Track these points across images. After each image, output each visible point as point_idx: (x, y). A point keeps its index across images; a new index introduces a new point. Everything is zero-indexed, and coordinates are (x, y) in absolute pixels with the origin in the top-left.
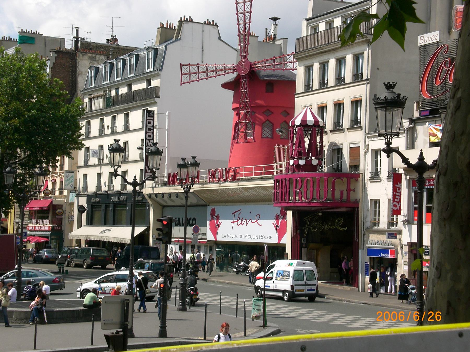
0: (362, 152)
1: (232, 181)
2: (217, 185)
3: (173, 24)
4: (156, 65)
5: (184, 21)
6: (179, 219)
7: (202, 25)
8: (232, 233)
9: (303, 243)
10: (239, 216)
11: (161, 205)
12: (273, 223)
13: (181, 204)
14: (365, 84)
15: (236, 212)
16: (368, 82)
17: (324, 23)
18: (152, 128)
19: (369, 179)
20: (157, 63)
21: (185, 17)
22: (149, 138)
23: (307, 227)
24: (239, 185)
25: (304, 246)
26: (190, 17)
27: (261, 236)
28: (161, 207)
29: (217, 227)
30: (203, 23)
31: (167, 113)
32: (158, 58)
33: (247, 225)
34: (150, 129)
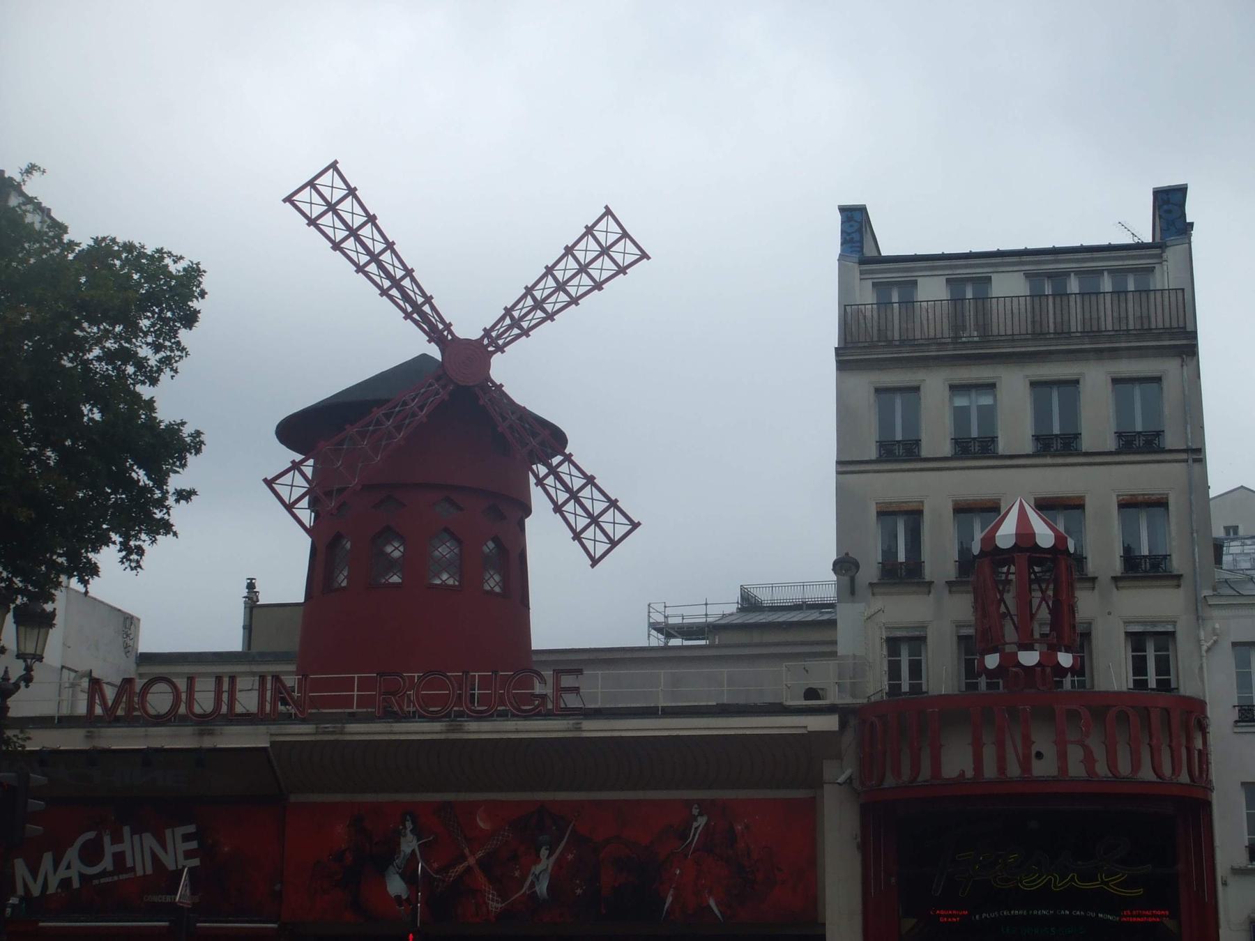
17: (944, 278)
24: (580, 729)
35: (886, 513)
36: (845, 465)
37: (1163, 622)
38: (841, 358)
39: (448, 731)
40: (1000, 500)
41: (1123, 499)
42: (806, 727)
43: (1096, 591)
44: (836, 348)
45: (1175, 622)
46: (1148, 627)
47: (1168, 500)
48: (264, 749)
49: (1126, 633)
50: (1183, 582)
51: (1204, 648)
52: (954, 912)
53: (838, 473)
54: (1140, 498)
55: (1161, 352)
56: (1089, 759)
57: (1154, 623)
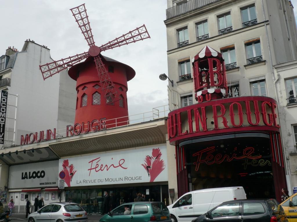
1: (96, 131)
2: (78, 137)
3: (17, 49)
4: (7, 66)
6: (26, 173)
7: (40, 47)
8: (88, 178)
9: (189, 178)
10: (97, 163)
11: (7, 164)
12: (143, 165)
13: (29, 161)
14: (264, 25)
15: (93, 160)
18: (5, 104)
21: (29, 39)
24: (106, 134)
25: (190, 181)
27: (126, 178)
30: (41, 46)
32: (10, 61)
33: (107, 170)
34: (3, 105)
35: (181, 63)
36: (169, 51)
38: (166, 23)
39: (80, 138)
42: (156, 125)
43: (240, 71)
44: (164, 21)
45: (265, 76)
48: (48, 147)
49: (250, 82)
52: (244, 174)
53: (168, 54)
54: (251, 41)
56: (225, 122)
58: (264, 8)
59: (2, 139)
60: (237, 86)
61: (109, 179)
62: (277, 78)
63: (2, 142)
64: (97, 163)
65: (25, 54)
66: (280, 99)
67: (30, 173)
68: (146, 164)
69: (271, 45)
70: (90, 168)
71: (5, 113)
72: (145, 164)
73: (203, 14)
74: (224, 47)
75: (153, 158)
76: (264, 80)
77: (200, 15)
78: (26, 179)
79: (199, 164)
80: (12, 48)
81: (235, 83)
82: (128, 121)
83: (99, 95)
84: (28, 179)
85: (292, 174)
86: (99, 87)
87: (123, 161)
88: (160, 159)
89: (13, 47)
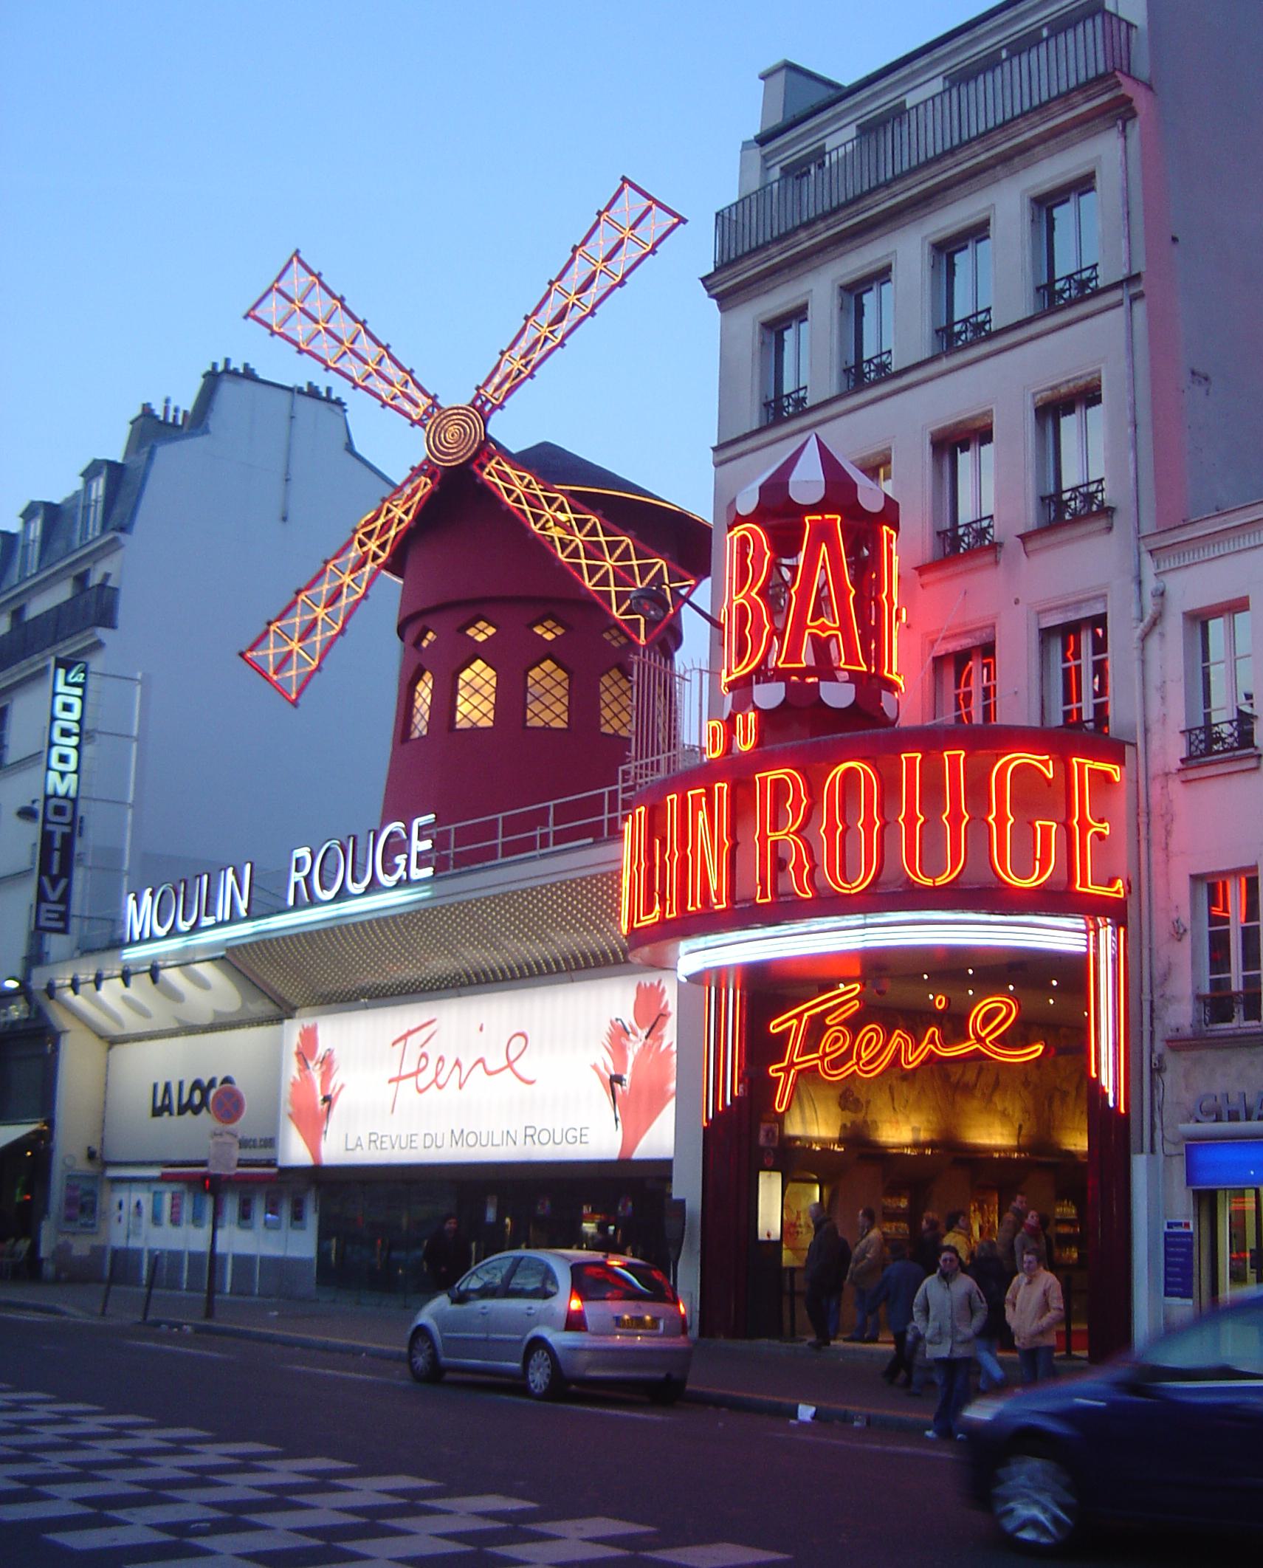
0: (1121, 636)
5: (226, 371)
6: (167, 1086)
7: (289, 394)
10: (424, 1049)
11: (101, 1037)
12: (595, 1067)
13: (174, 1025)
14: (1119, 304)
15: (410, 1033)
16: (1134, 290)
18: (75, 729)
19: (1179, 765)
20: (117, 511)
21: (227, 361)
22: (62, 767)
23: (792, 1064)
26: (246, 366)
28: (100, 1047)
29: (322, 1107)
31: (139, 676)
33: (461, 1086)
36: (726, 450)
37: (1088, 600)
38: (714, 292)
40: (890, 449)
41: (1042, 398)
44: (703, 280)
45: (1105, 595)
46: (1069, 614)
47: (1100, 381)
48: (222, 958)
49: (1041, 630)
50: (1117, 520)
51: (1138, 633)
53: (718, 464)
54: (1063, 390)
55: (1086, 125)
57: (1078, 604)
58: (1127, 203)
59: (61, 908)
60: (987, 650)
61: (465, 1133)
62: (1150, 610)
63: (60, 925)
64: (424, 1049)
65: (198, 443)
66: (1155, 728)
67: (181, 1084)
68: (610, 1065)
69: (1144, 416)
70: (396, 1074)
71: (75, 772)
72: (606, 1068)
73: (876, 233)
74: (949, 426)
75: (636, 1034)
76: (1100, 620)
77: (858, 241)
78: (166, 1114)
79: (793, 1071)
80: (159, 412)
81: (978, 634)
82: (538, 832)
83: (489, 673)
84: (175, 1118)
85: (1170, 1149)
86: (491, 631)
87: (521, 1040)
88: (661, 1037)
89: (167, 401)
